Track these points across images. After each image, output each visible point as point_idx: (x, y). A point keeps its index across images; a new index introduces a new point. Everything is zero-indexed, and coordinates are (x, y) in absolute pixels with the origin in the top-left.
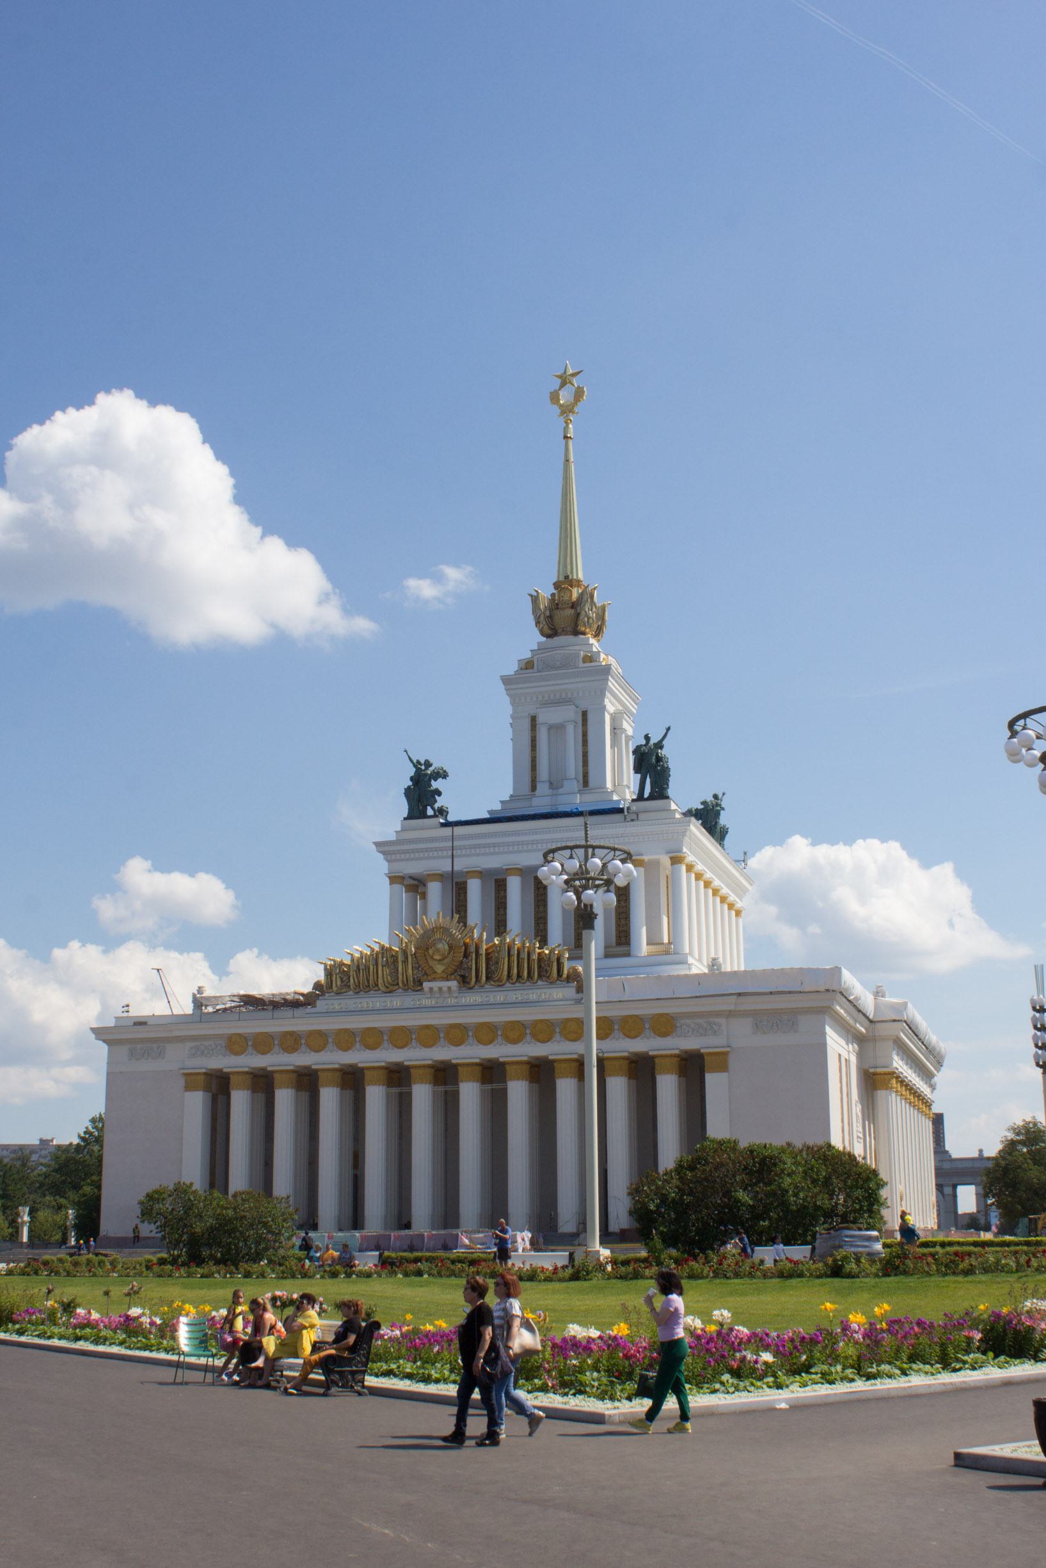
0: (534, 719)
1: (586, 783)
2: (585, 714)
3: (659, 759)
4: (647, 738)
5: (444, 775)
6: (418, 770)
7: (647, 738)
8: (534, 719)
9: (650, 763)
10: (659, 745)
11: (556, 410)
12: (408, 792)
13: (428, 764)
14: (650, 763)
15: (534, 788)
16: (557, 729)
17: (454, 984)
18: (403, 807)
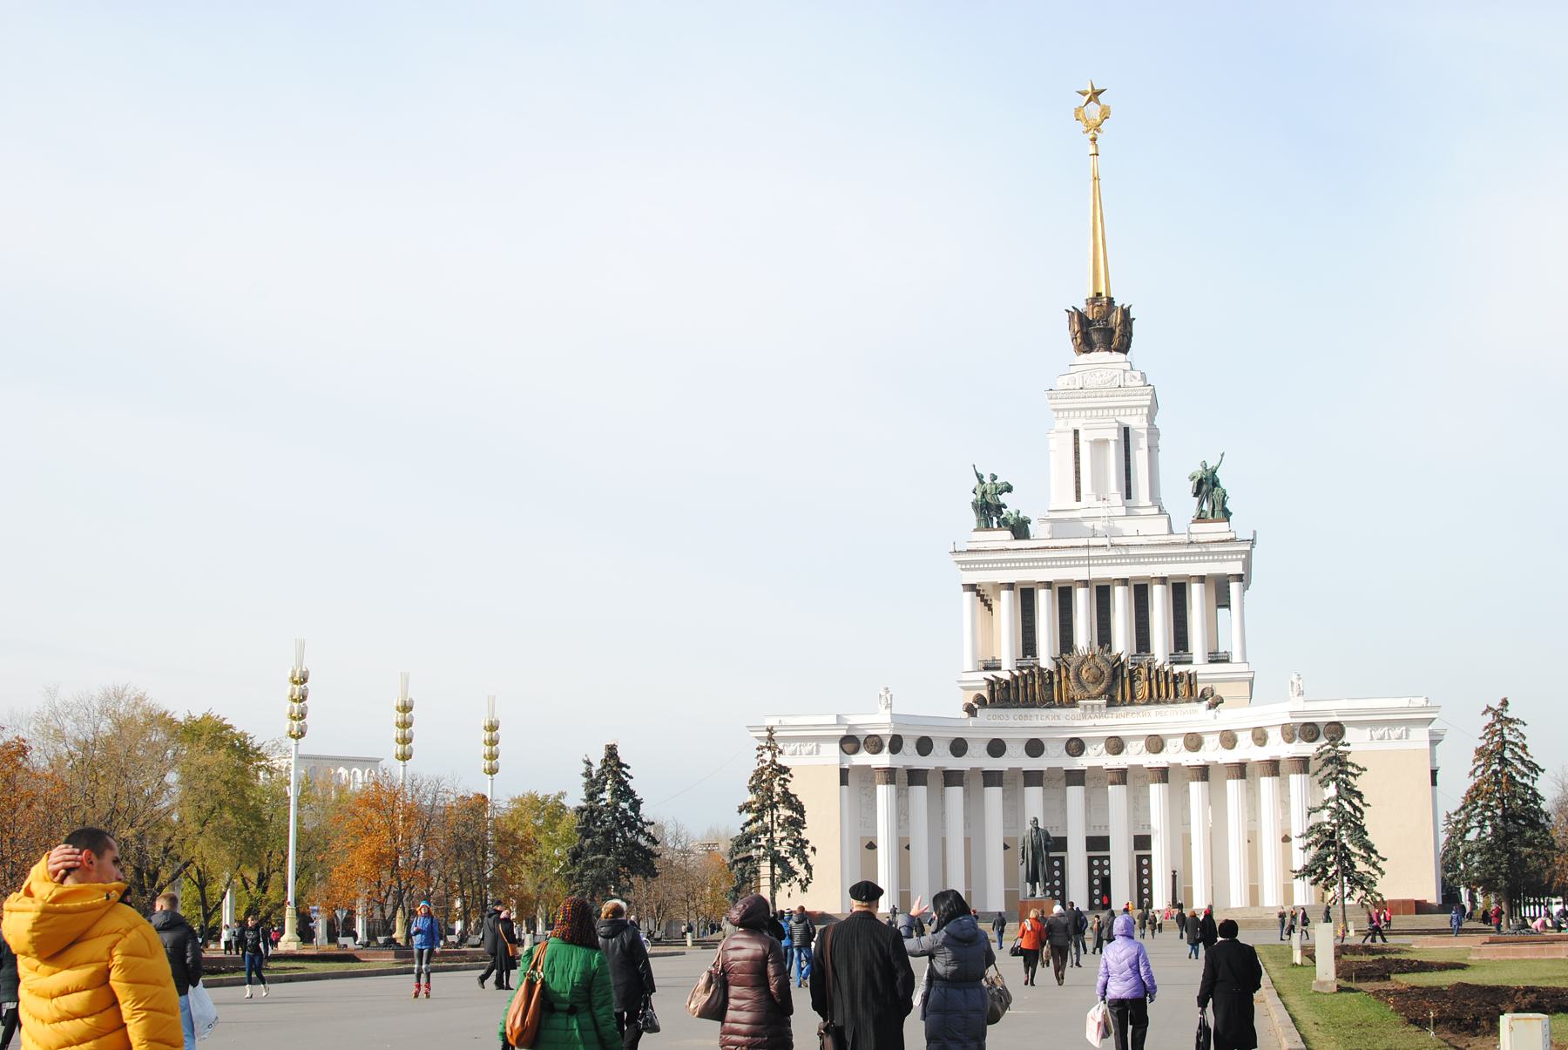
0: (1076, 432)
1: (1129, 496)
2: (1126, 430)
3: (1215, 484)
4: (1204, 464)
5: (1009, 489)
6: (982, 482)
7: (1204, 464)
8: (1076, 432)
9: (1206, 485)
10: (1214, 473)
11: (1081, 126)
12: (975, 506)
13: (994, 477)
14: (1206, 485)
15: (1078, 498)
16: (1100, 444)
17: (1103, 702)
18: (972, 518)
